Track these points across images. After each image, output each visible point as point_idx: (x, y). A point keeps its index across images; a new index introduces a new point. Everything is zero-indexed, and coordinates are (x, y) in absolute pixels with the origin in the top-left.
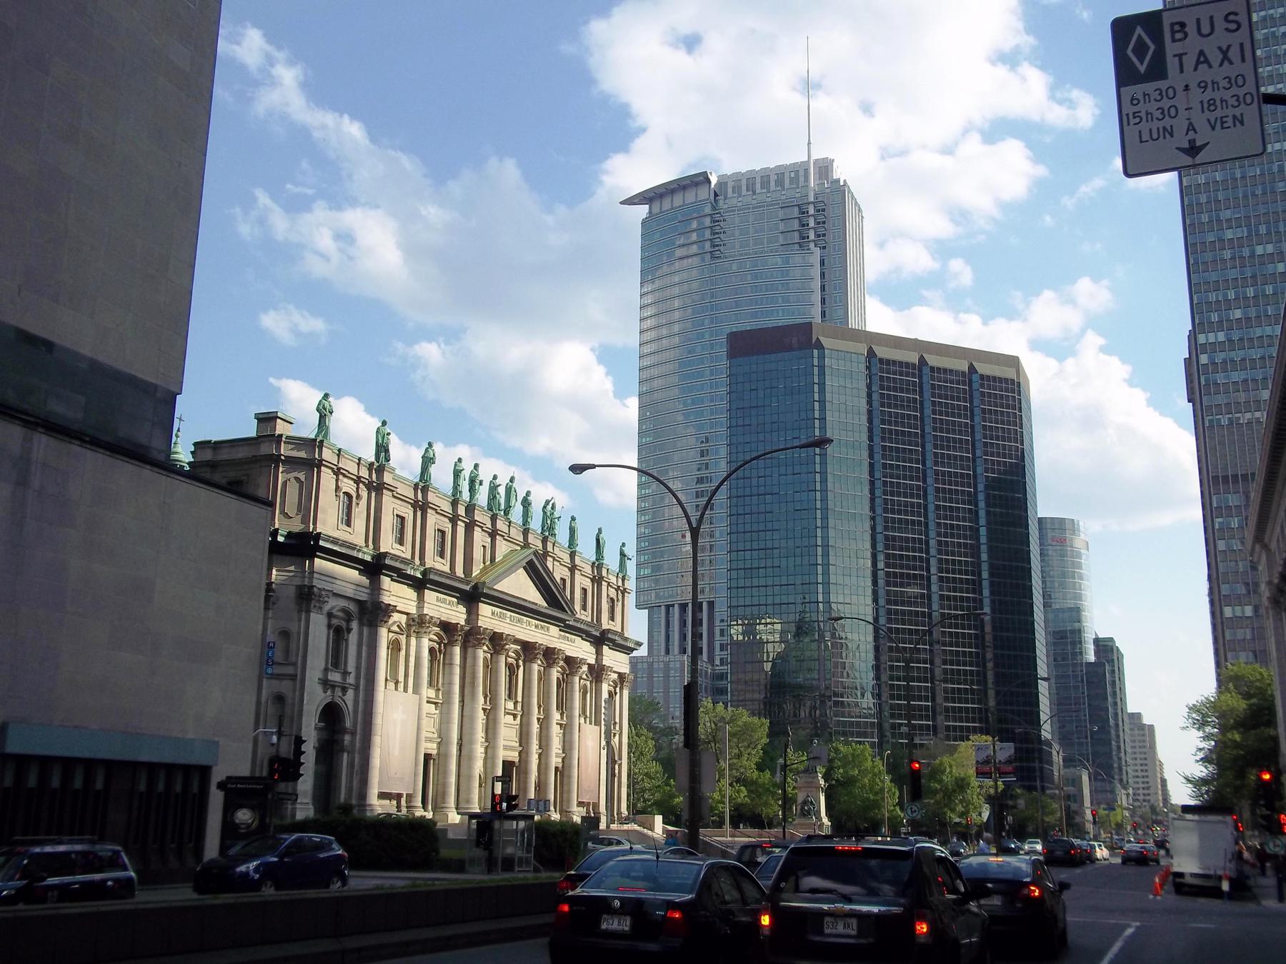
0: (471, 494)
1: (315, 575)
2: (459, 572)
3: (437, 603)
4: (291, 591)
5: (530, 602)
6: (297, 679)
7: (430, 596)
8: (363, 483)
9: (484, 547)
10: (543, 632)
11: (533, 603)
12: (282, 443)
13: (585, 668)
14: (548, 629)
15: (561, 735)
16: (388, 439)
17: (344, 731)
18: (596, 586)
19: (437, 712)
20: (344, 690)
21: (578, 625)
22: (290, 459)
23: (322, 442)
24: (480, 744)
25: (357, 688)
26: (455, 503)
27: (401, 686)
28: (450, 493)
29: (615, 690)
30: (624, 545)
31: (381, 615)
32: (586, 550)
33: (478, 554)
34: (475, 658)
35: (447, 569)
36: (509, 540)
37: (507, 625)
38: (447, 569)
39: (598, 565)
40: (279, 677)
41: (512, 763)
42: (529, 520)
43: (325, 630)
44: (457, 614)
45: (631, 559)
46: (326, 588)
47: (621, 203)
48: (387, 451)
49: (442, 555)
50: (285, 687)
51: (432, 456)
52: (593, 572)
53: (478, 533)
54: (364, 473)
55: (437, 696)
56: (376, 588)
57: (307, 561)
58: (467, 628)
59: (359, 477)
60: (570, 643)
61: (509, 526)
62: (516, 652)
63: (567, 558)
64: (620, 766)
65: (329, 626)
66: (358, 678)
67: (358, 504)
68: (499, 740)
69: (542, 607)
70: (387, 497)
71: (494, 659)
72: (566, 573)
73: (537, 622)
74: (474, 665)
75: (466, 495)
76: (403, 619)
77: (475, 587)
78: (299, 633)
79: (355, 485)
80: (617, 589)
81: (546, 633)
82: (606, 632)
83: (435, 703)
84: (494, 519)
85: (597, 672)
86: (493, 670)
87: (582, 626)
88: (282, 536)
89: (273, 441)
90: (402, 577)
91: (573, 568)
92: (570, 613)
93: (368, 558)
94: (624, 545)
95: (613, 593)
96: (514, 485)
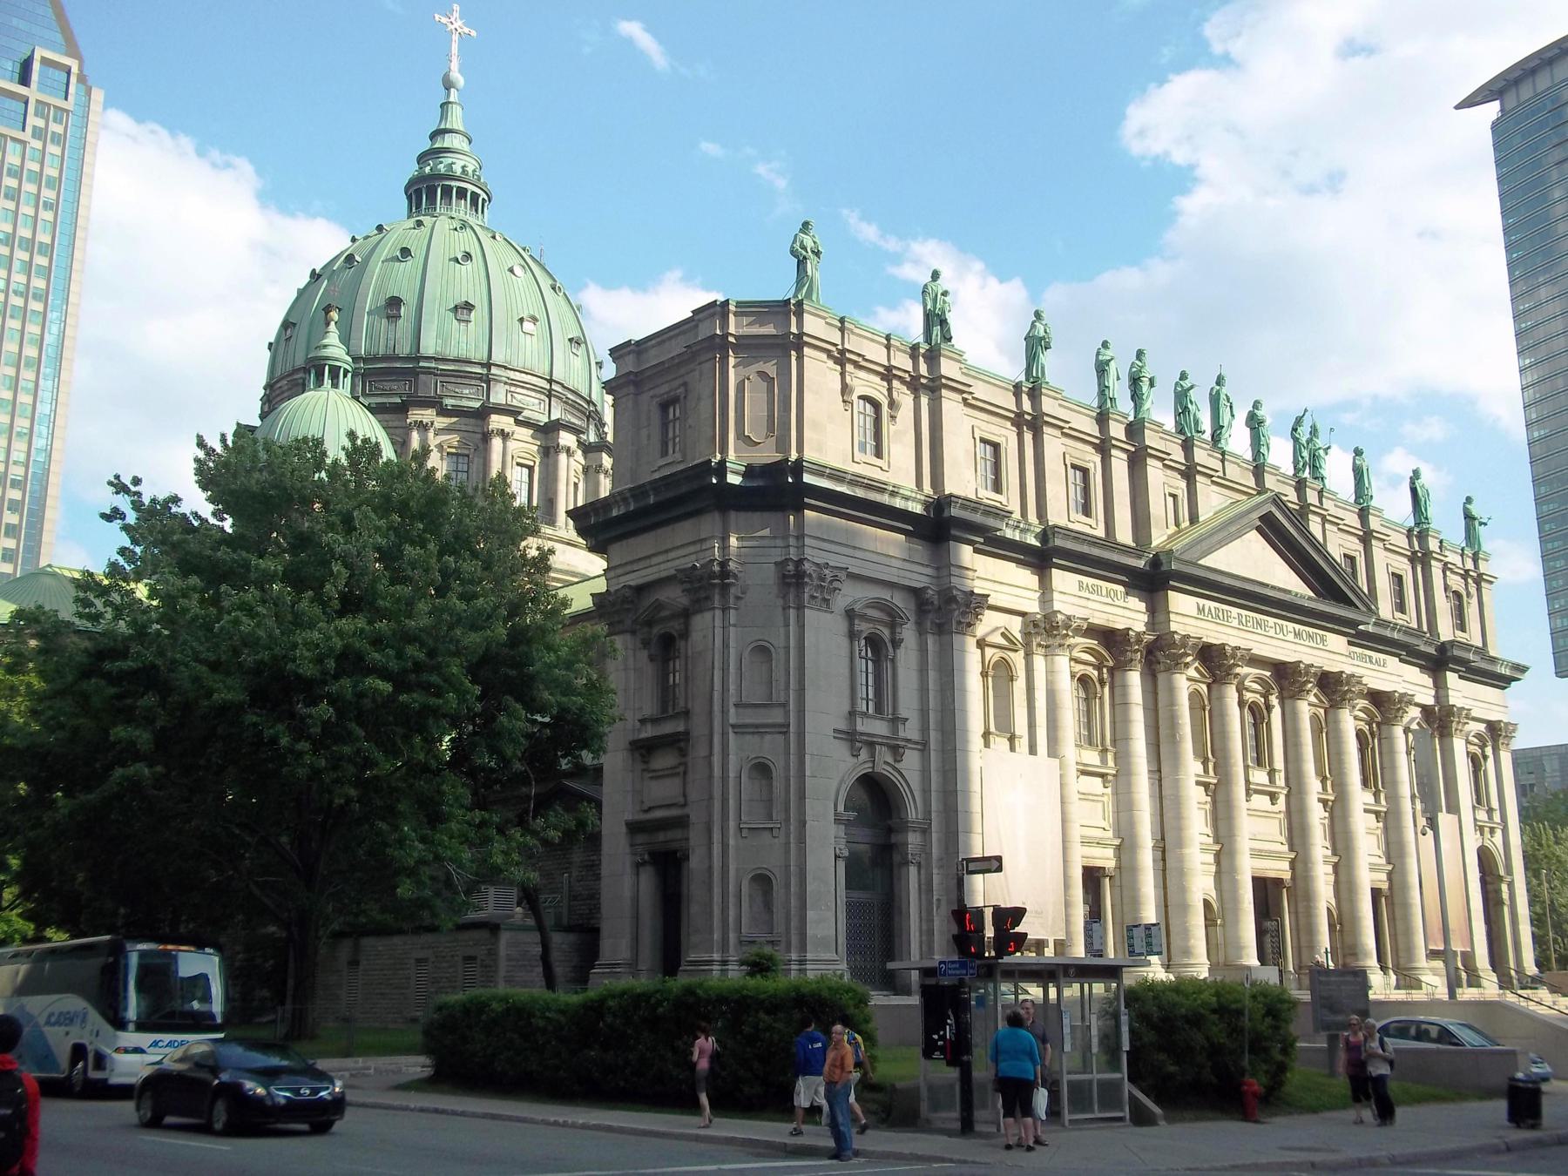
0: (1136, 405)
1: (807, 541)
2: (1124, 535)
3: (1082, 594)
4: (769, 574)
5: (1274, 588)
6: (790, 731)
7: (1062, 579)
8: (900, 378)
9: (1174, 496)
10: (1311, 644)
11: (1280, 590)
12: (731, 316)
13: (1414, 712)
14: (1323, 640)
15: (1379, 832)
16: (944, 302)
17: (904, 827)
18: (1419, 569)
19: (1109, 791)
20: (896, 751)
21: (1388, 633)
22: (745, 342)
23: (800, 304)
24: (1199, 846)
25: (923, 746)
26: (1102, 419)
27: (1023, 744)
28: (1095, 404)
29: (1483, 752)
30: (1469, 500)
31: (956, 613)
32: (1393, 507)
33: (1158, 505)
34: (1171, 690)
35: (1100, 532)
36: (1224, 484)
37: (1235, 632)
38: (1100, 532)
39: (1419, 531)
40: (758, 730)
41: (1278, 882)
42: (1263, 450)
43: (845, 642)
44: (1129, 614)
45: (1485, 524)
46: (831, 564)
47: (1457, 107)
48: (943, 322)
49: (1086, 510)
50: (768, 748)
51: (1042, 333)
52: (1411, 544)
53: (1154, 471)
54: (903, 361)
55: (1104, 761)
56: (944, 566)
57: (792, 517)
58: (1149, 638)
59: (889, 368)
60: (1376, 667)
61: (1223, 461)
62: (1260, 680)
63: (1352, 520)
64: (1511, 885)
65: (852, 635)
66: (925, 729)
67: (893, 417)
68: (1239, 839)
69: (1302, 597)
70: (951, 405)
71: (1214, 693)
72: (1355, 547)
73: (1298, 627)
74: (1172, 703)
75: (1125, 405)
76: (1015, 625)
77: (1156, 562)
78: (787, 648)
79: (885, 384)
80: (1465, 575)
81: (1321, 646)
82: (1448, 647)
83: (1102, 776)
84: (1187, 446)
85: (1440, 719)
86: (1215, 713)
87: (1396, 636)
88: (736, 473)
89: (713, 315)
90: (999, 547)
91: (1366, 538)
92: (1363, 609)
93: (918, 509)
94: (1469, 500)
95: (1456, 582)
96: (1224, 391)
